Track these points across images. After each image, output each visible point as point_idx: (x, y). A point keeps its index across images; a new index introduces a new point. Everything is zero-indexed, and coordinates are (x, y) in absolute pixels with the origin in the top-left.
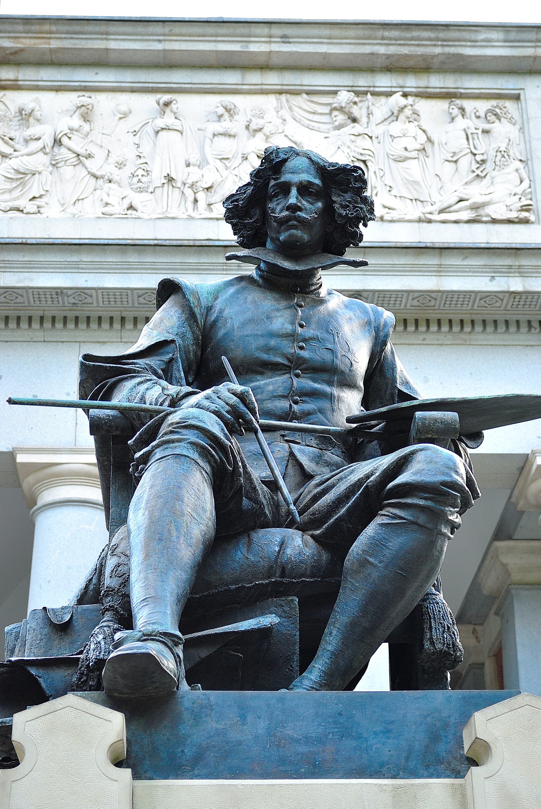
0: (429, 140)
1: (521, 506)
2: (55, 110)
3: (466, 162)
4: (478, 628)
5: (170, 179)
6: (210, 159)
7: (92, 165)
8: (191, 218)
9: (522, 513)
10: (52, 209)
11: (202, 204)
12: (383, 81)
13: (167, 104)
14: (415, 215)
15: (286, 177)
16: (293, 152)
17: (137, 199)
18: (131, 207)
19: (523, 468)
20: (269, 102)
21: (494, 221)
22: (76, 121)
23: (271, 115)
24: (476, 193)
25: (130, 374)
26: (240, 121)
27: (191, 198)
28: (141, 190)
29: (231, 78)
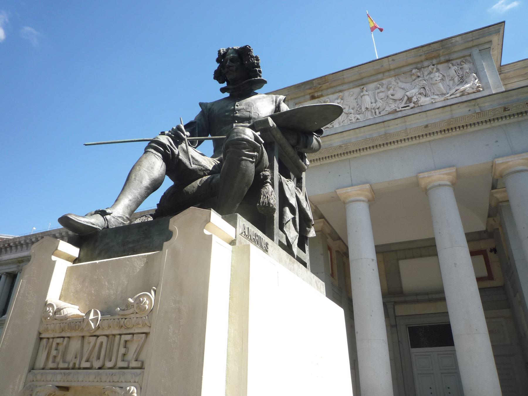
0: (443, 76)
3: (456, 79)
5: (367, 108)
6: (378, 100)
8: (375, 118)
9: (497, 180)
11: (377, 113)
12: (426, 64)
13: (363, 88)
14: (443, 99)
17: (358, 116)
18: (358, 119)
21: (469, 94)
23: (394, 83)
26: (385, 86)
27: (374, 112)
28: (359, 114)
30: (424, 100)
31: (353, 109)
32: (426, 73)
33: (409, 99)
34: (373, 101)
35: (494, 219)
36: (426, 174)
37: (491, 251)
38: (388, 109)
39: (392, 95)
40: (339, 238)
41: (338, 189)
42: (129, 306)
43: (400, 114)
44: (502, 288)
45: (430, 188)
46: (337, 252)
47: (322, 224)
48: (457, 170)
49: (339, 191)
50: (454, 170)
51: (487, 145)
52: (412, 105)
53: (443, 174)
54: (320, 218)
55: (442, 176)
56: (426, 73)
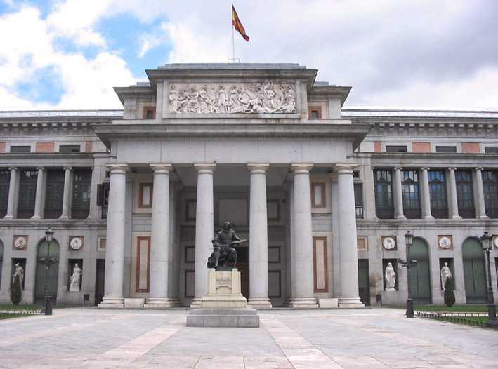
2: (199, 86)
5: (222, 104)
7: (207, 101)
10: (199, 112)
12: (267, 81)
20: (243, 85)
22: (203, 91)
24: (284, 107)
29: (235, 80)
30: (261, 109)
31: (212, 101)
32: (265, 88)
33: (251, 106)
34: (227, 99)
38: (236, 109)
39: (241, 99)
43: (243, 116)
51: (290, 152)
52: (252, 111)
56: (265, 88)
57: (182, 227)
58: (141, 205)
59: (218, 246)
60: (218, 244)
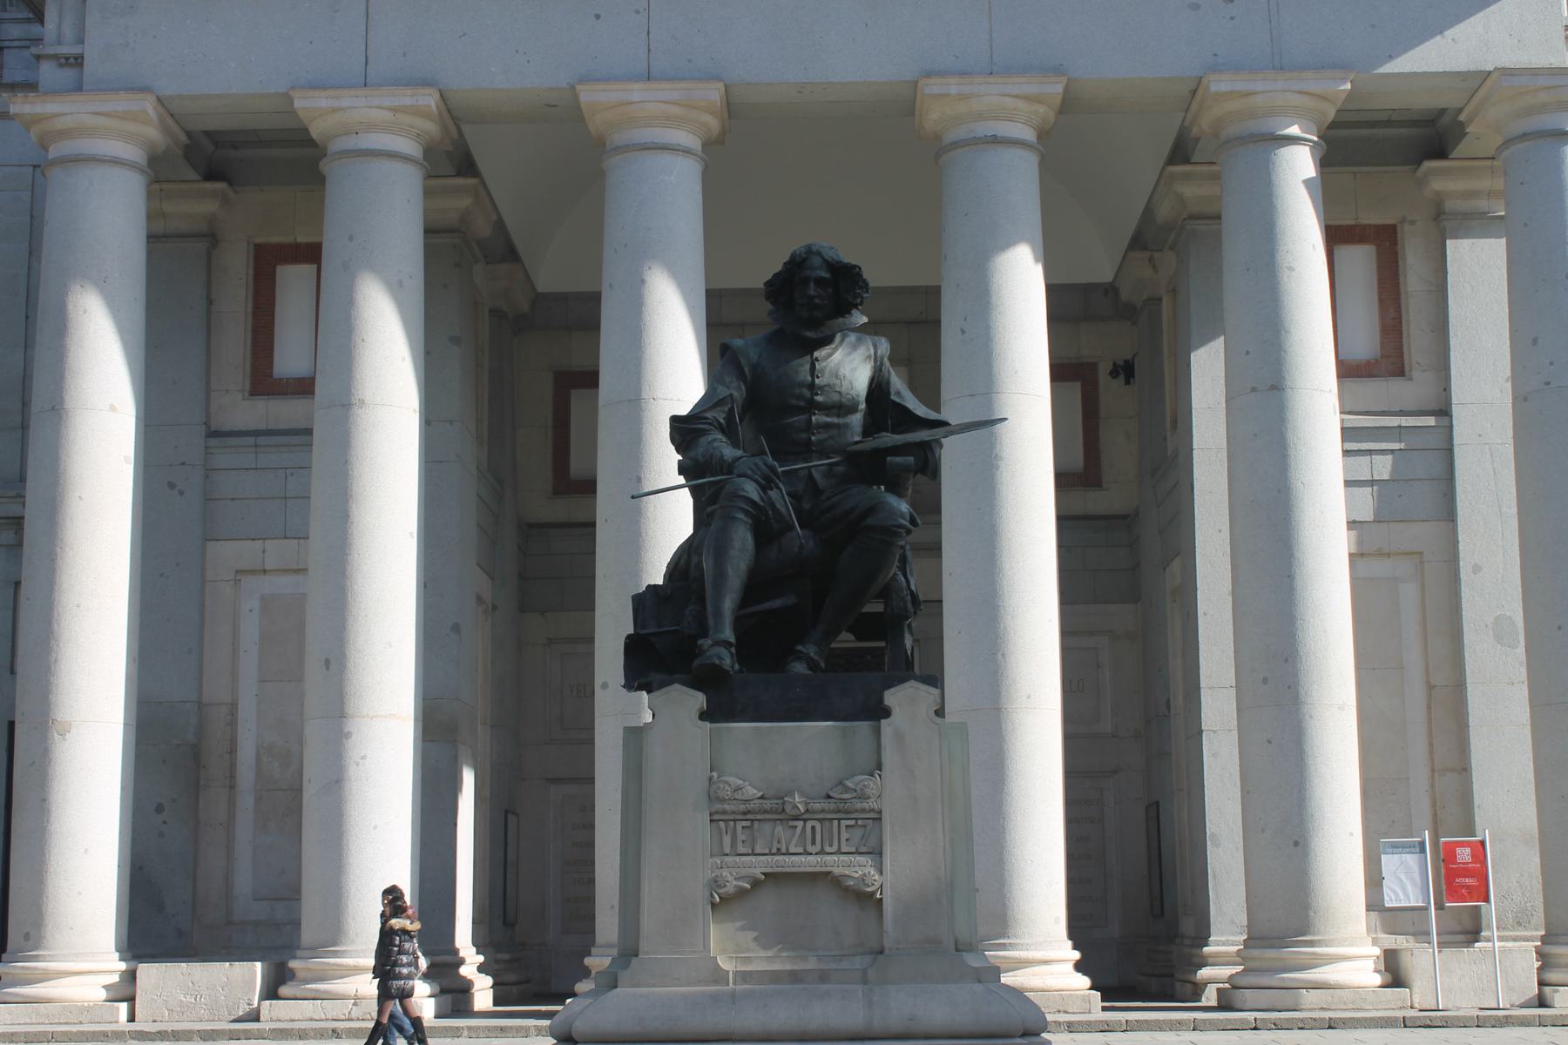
1: (1195, 131)
4: (1157, 255)
9: (1197, 140)
15: (808, 272)
16: (809, 251)
19: (1194, 92)
25: (703, 433)
35: (1151, 259)
36: (953, 86)
37: (1114, 373)
40: (512, 254)
41: (582, 80)
42: (847, 790)
44: (1122, 523)
45: (956, 145)
46: (494, 312)
47: (465, 202)
48: (1066, 90)
49: (589, 96)
50: (1059, 88)
53: (1016, 96)
54: (459, 174)
55: (1009, 101)
57: (530, 530)
58: (264, 382)
59: (728, 468)
60: (729, 452)
